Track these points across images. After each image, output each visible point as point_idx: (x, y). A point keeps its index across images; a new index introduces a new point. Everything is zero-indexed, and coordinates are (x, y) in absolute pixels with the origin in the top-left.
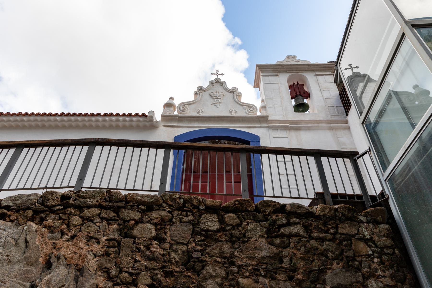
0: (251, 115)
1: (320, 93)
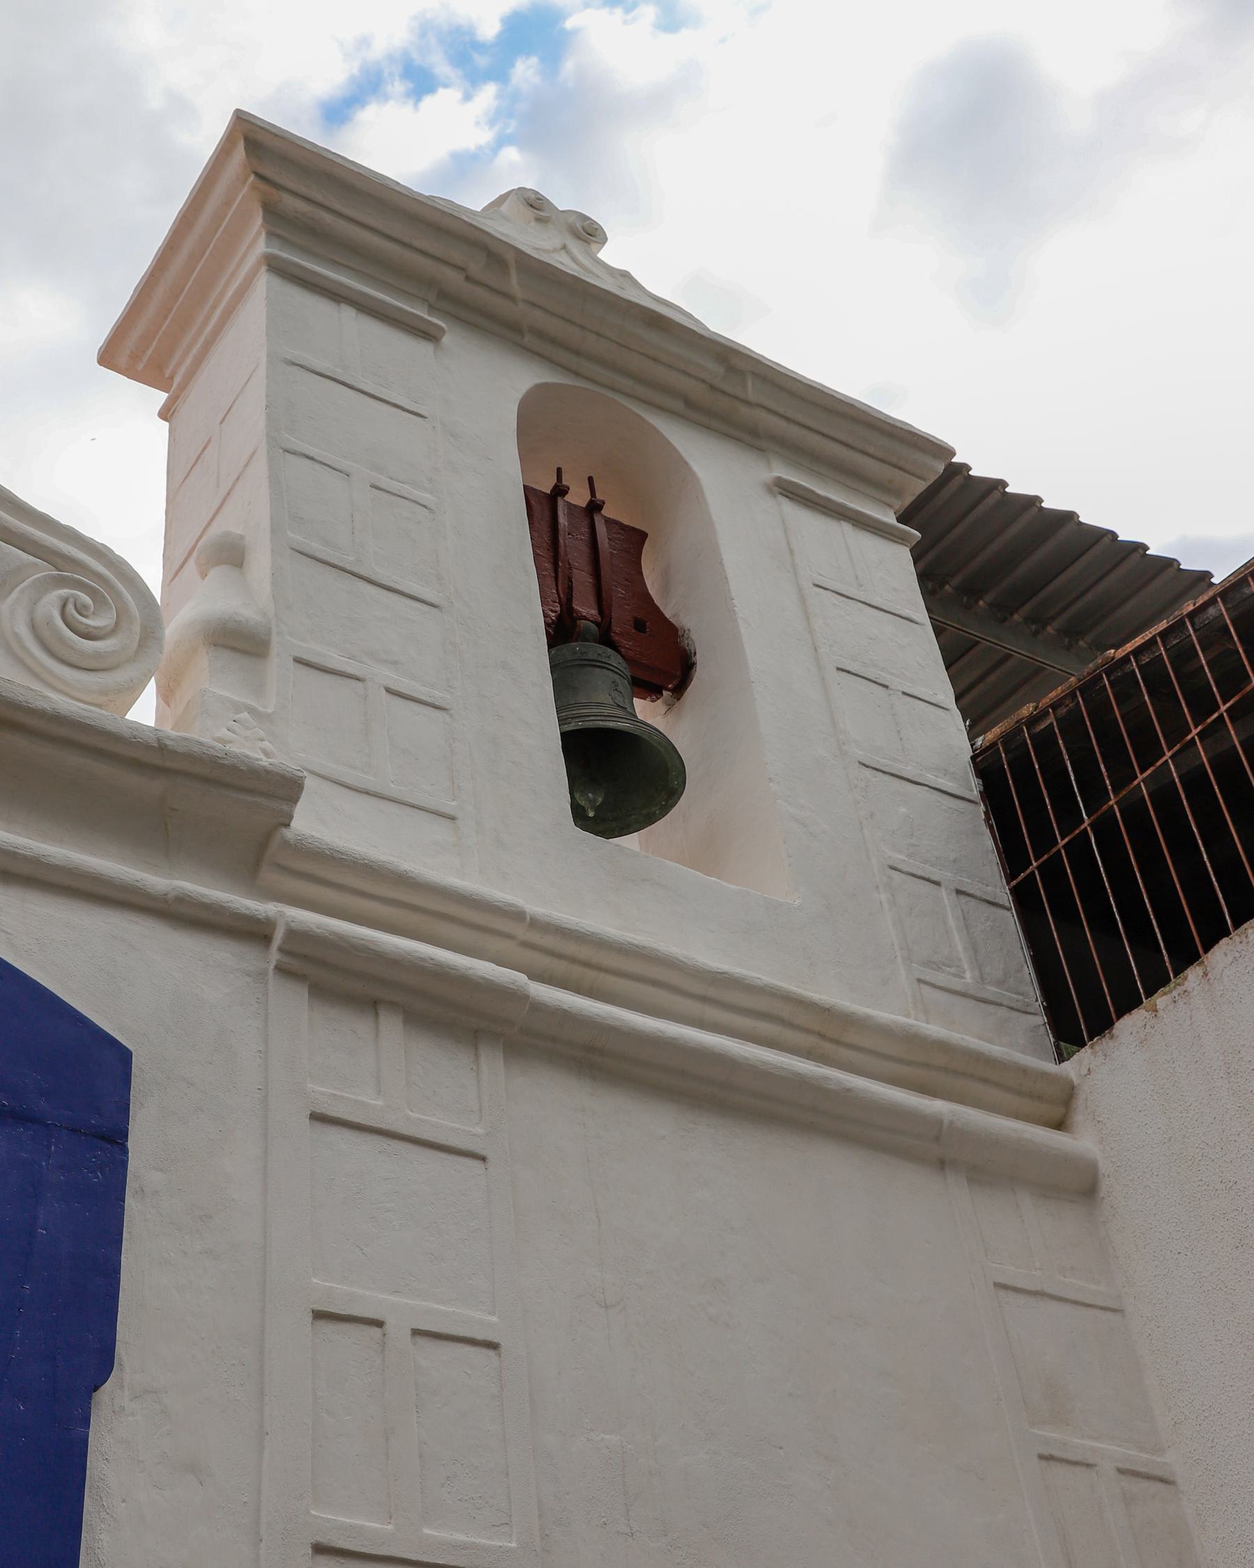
0: (62, 694)
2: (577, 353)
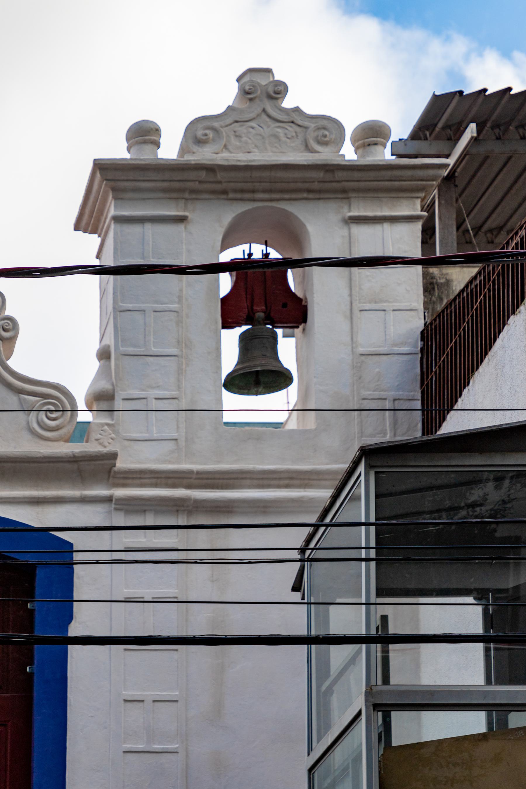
1: (345, 326)
2: (254, 191)
